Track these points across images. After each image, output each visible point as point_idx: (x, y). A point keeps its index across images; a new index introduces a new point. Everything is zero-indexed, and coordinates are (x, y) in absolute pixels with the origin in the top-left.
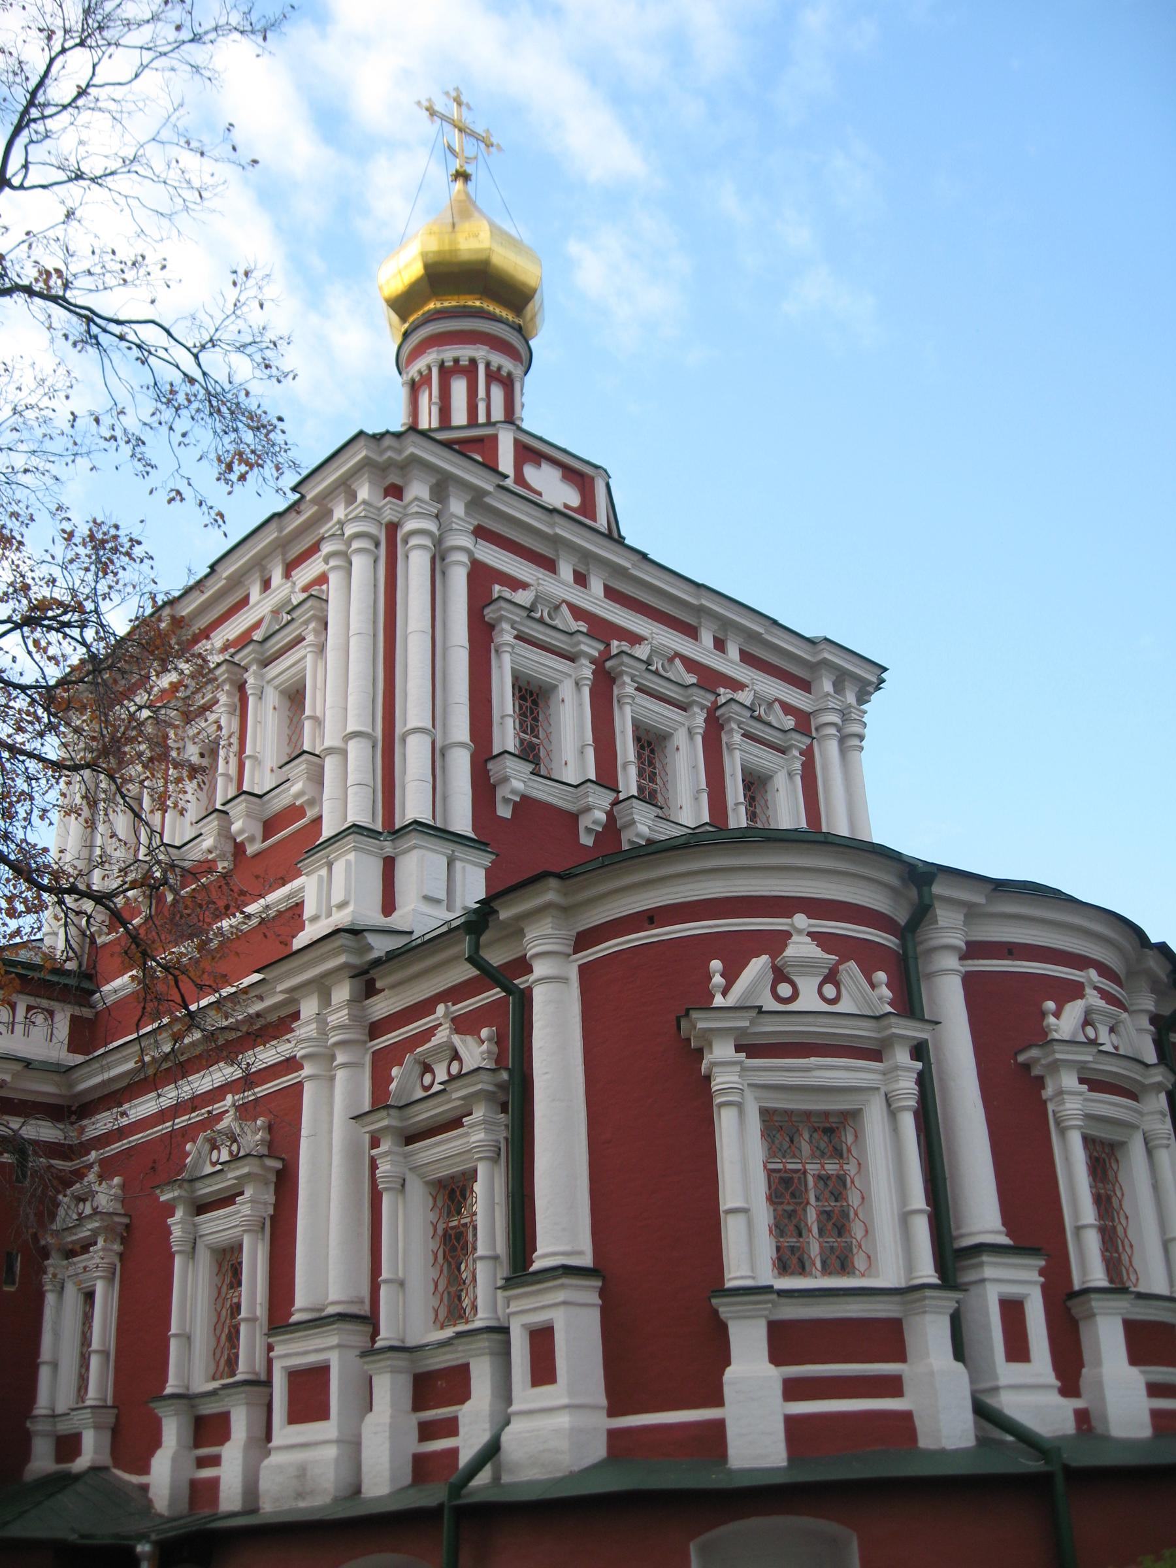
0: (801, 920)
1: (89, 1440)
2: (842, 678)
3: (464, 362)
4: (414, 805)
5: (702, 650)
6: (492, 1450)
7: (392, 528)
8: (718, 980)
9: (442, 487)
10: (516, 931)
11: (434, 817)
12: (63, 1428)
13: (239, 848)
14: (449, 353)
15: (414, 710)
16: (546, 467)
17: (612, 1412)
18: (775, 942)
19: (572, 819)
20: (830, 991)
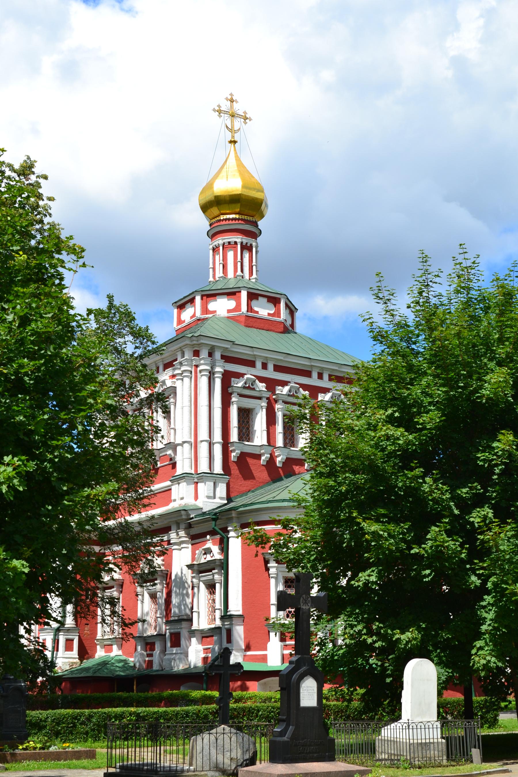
16: (260, 298)
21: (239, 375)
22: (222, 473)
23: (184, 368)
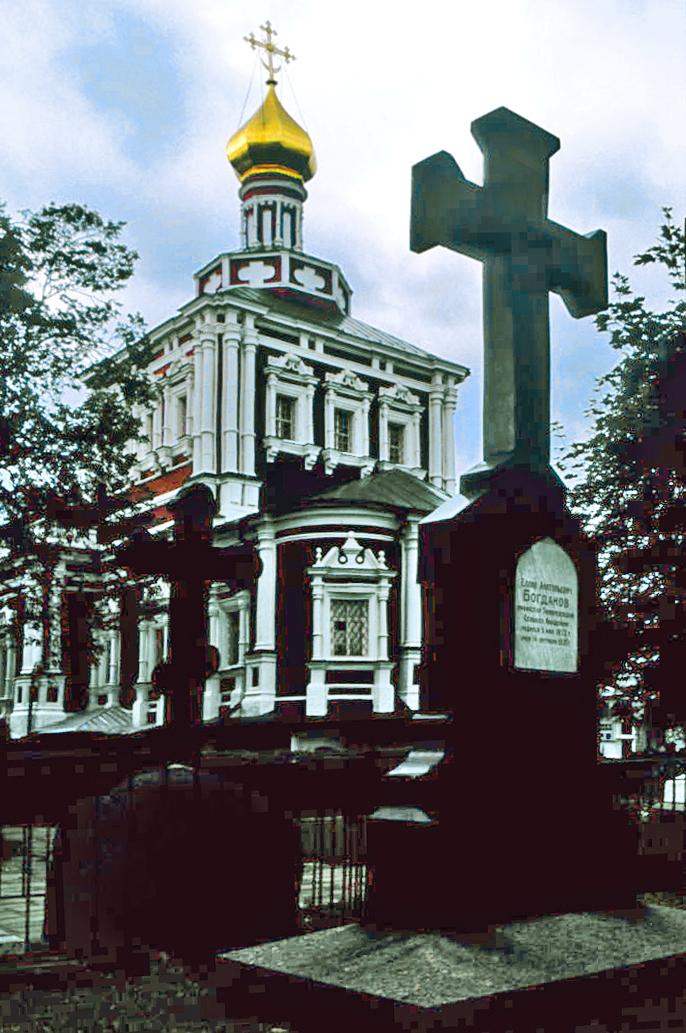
0: (351, 534)
1: (110, 697)
2: (446, 375)
4: (229, 466)
5: (373, 371)
6: (239, 706)
7: (220, 336)
8: (319, 556)
9: (242, 315)
10: (254, 529)
11: (238, 468)
12: (101, 692)
13: (163, 469)
14: (263, 199)
15: (229, 423)
17: (277, 695)
18: (341, 542)
19: (301, 460)
20: (360, 559)
21: (278, 354)
22: (254, 475)
23: (203, 337)
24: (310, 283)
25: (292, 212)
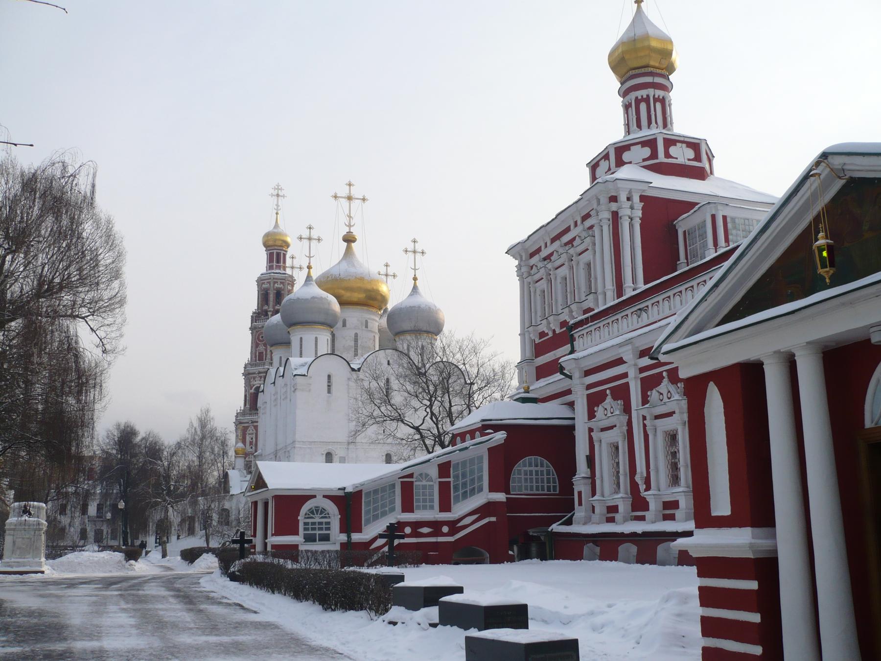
3: (645, 97)
24: (682, 155)
25: (663, 101)
